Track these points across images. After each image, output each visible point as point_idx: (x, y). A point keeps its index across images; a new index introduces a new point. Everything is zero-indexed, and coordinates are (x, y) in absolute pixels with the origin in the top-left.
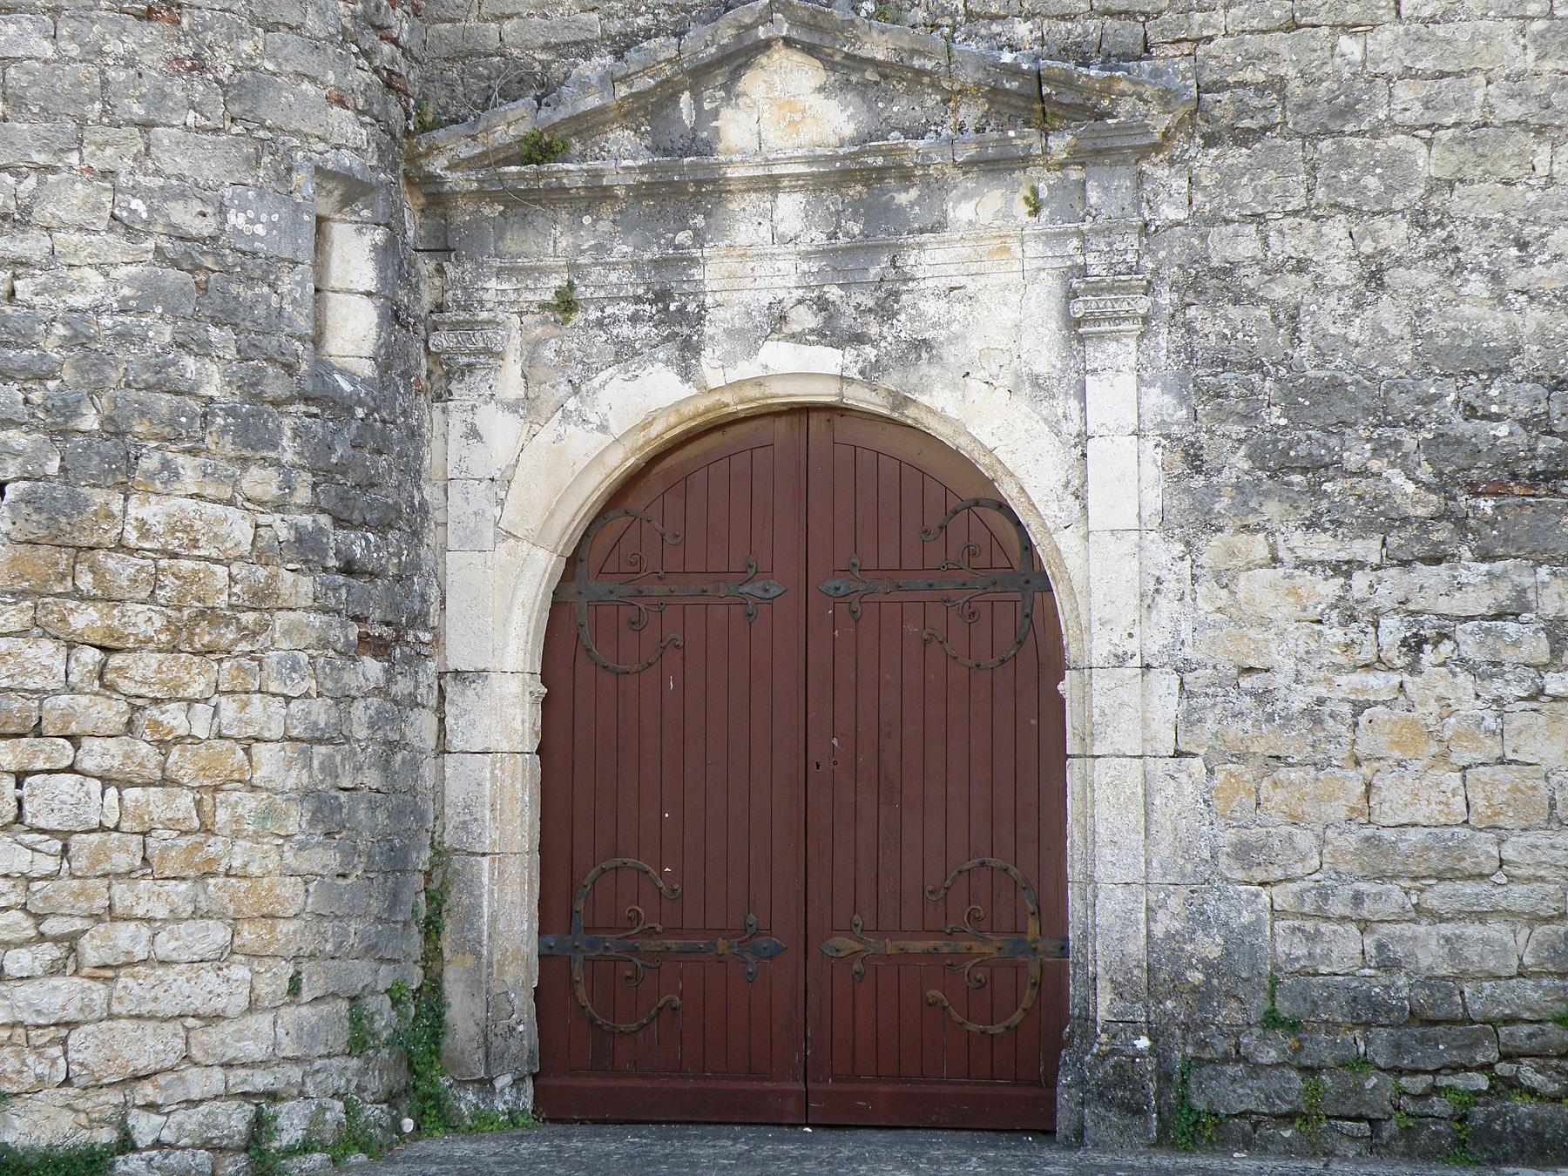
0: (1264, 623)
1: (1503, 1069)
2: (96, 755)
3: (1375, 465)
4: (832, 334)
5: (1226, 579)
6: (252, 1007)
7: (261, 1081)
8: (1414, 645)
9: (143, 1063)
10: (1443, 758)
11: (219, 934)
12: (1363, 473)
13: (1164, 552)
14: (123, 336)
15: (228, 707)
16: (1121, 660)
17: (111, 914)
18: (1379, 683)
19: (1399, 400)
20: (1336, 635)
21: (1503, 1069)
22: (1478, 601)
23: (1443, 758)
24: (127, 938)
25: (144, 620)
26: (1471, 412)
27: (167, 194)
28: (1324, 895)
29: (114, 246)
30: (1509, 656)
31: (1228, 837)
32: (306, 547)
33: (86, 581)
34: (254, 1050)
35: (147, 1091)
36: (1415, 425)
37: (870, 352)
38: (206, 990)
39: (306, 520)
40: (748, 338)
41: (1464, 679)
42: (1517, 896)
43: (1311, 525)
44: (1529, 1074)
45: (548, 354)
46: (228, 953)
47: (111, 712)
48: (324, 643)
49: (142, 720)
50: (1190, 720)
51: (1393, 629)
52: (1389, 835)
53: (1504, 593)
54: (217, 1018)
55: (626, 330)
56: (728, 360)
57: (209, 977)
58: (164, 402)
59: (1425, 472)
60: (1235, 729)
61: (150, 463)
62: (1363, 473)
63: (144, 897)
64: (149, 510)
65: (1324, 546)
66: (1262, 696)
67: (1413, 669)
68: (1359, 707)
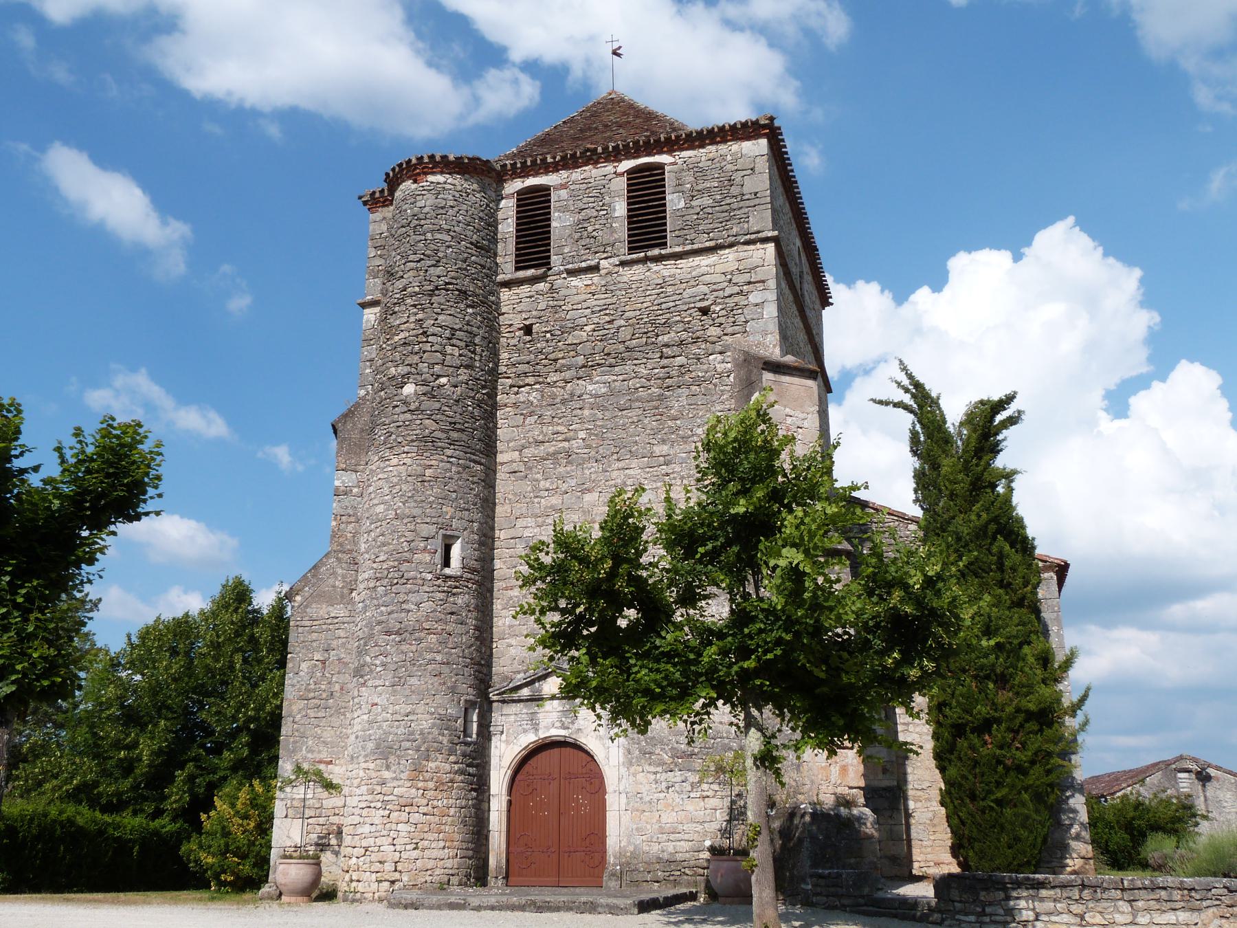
0: (641, 784)
1: (683, 870)
3: (661, 753)
4: (564, 727)
5: (634, 775)
6: (449, 858)
8: (668, 788)
9: (429, 867)
10: (673, 810)
11: (442, 844)
12: (659, 754)
13: (623, 770)
14: (429, 733)
15: (445, 801)
16: (615, 791)
18: (662, 795)
19: (665, 740)
20: (654, 786)
21: (683, 870)
22: (679, 779)
23: (673, 810)
24: (426, 843)
25: (431, 785)
26: (677, 743)
27: (438, 707)
28: (652, 837)
29: (428, 716)
30: (684, 790)
31: (635, 827)
32: (461, 772)
33: (421, 778)
36: (668, 745)
37: (570, 731)
38: (441, 854)
40: (548, 728)
41: (676, 794)
42: (686, 836)
43: (650, 764)
44: (687, 871)
45: (511, 731)
46: (444, 848)
47: (424, 802)
49: (430, 803)
50: (628, 804)
51: (664, 785)
52: (663, 825)
53: (683, 778)
55: (525, 727)
56: (544, 732)
57: (441, 852)
59: (670, 755)
60: (636, 805)
62: (659, 754)
63: (430, 836)
64: (432, 765)
65: (652, 769)
66: (641, 799)
67: (668, 793)
68: (658, 800)
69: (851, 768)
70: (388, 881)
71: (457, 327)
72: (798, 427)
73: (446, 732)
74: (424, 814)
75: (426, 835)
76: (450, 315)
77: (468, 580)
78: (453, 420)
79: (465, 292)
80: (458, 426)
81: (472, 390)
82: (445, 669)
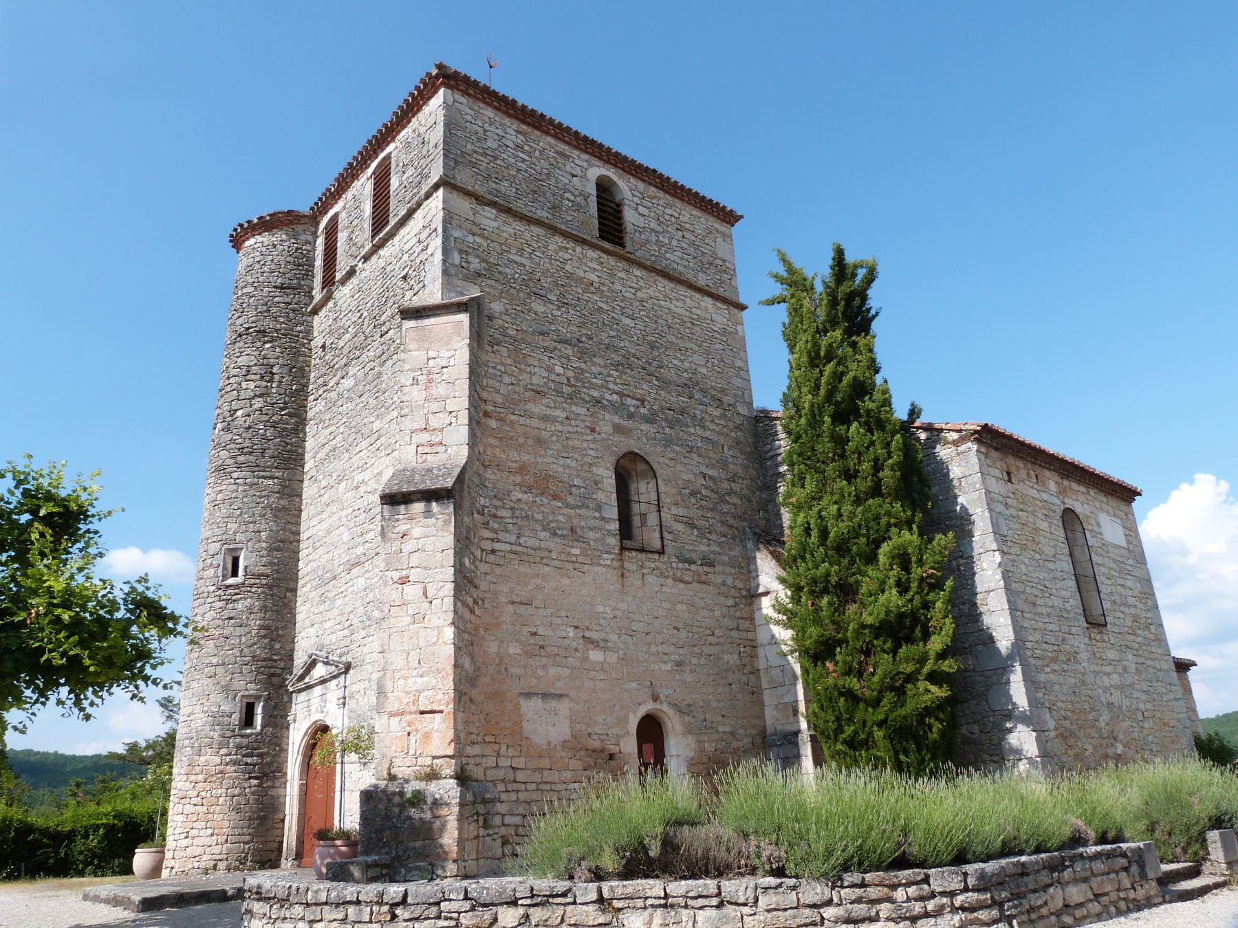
2: (194, 801)
11: (209, 831)
25: (201, 777)
29: (202, 715)
32: (235, 763)
38: (209, 841)
46: (212, 835)
57: (209, 839)
63: (199, 825)
64: (202, 759)
69: (435, 735)
71: (251, 364)
72: (443, 368)
73: (217, 727)
74: (195, 805)
75: (195, 825)
77: (251, 586)
78: (241, 446)
79: (265, 331)
80: (246, 450)
81: (267, 414)
82: (220, 670)
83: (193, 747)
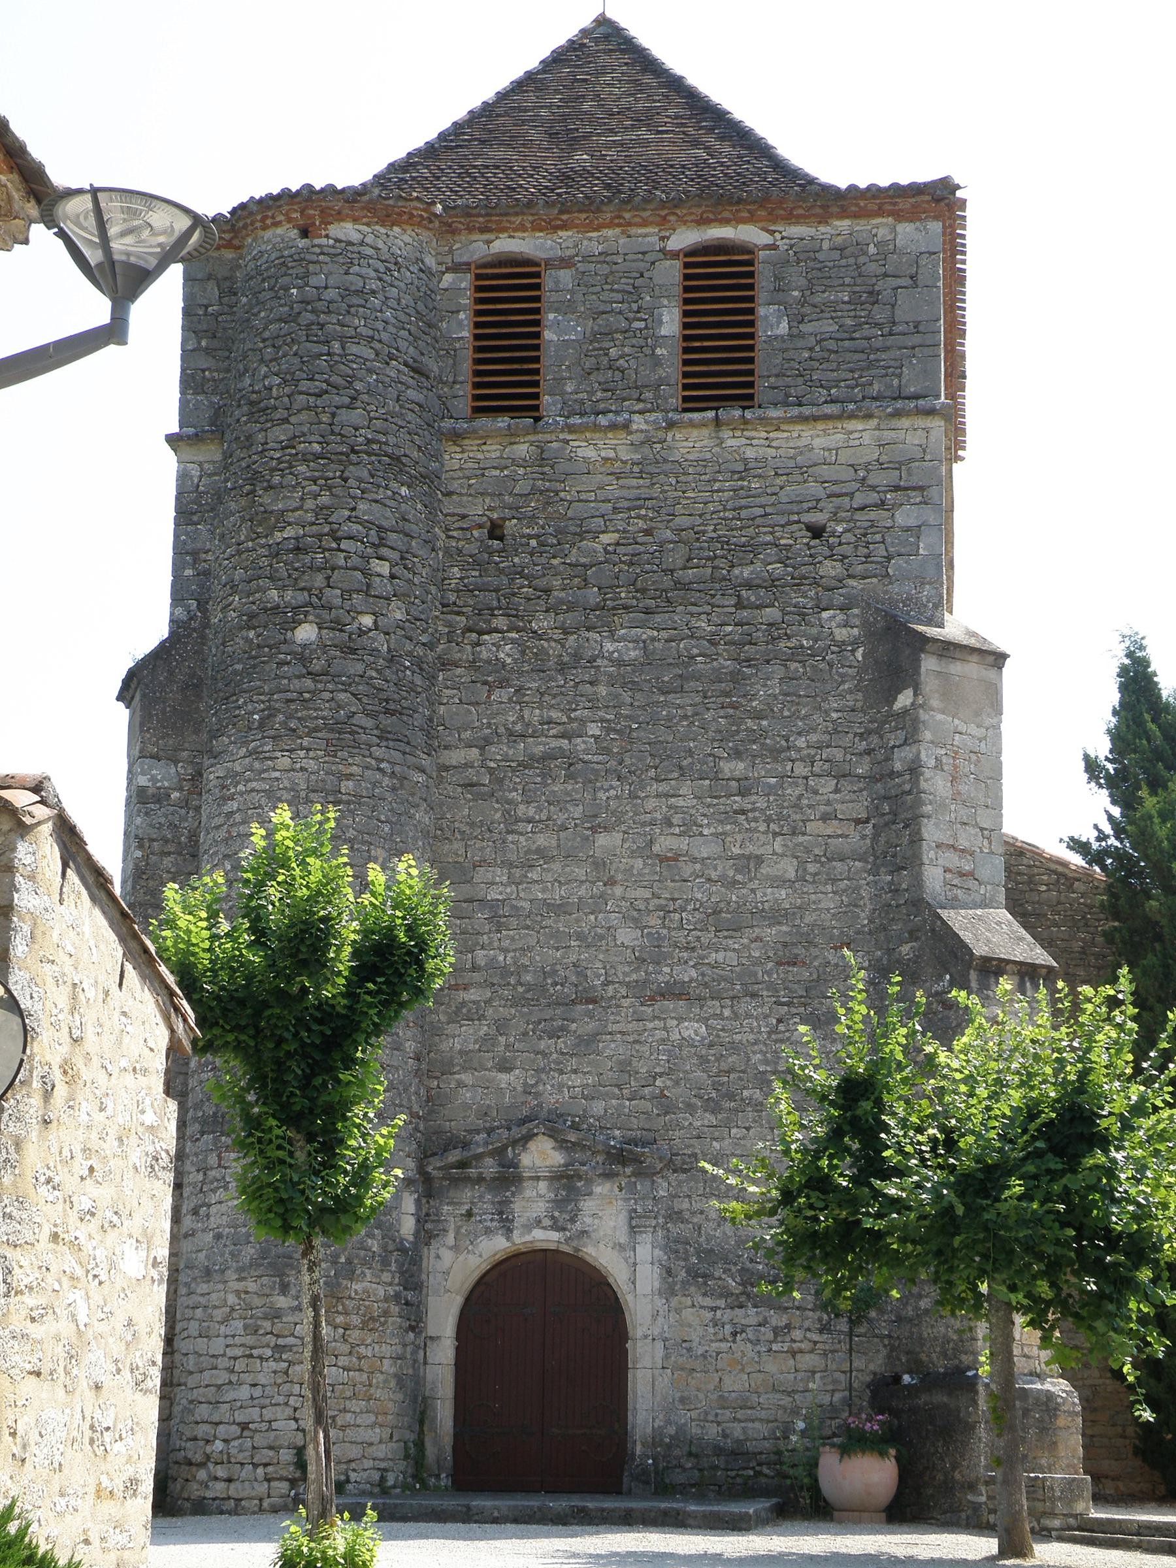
0: (690, 1326)
1: (758, 1468)
2: (343, 1361)
3: (723, 1276)
4: (556, 1227)
5: (678, 1311)
7: (383, 1465)
8: (734, 1334)
9: (352, 1456)
10: (742, 1370)
12: (720, 1279)
13: (660, 1302)
15: (377, 1347)
16: (646, 1337)
17: (345, 1410)
18: (724, 1346)
19: (731, 1256)
20: (711, 1330)
21: (758, 1468)
22: (753, 1320)
23: (742, 1370)
24: (349, 1417)
25: (355, 1320)
26: (751, 1261)
28: (706, 1414)
30: (762, 1338)
31: (679, 1394)
33: (340, 1308)
34: (381, 1455)
35: (353, 1465)
36: (735, 1264)
37: (568, 1234)
39: (397, 1288)
40: (528, 1228)
41: (749, 1345)
42: (763, 1414)
43: (705, 1295)
44: (765, 1470)
45: (463, 1231)
47: (346, 1348)
48: (401, 1327)
49: (354, 1351)
50: (667, 1357)
51: (728, 1329)
52: (726, 1395)
53: (761, 1319)
54: (371, 1444)
55: (489, 1224)
56: (523, 1234)
58: (362, 1253)
59: (738, 1279)
60: (681, 1360)
61: (358, 1272)
62: (720, 1279)
63: (355, 1406)
65: (708, 1302)
66: (689, 1350)
67: (734, 1341)
68: (718, 1354)
70: (287, 1480)
76: (376, 501)
78: (384, 695)
83: (335, 1263)
